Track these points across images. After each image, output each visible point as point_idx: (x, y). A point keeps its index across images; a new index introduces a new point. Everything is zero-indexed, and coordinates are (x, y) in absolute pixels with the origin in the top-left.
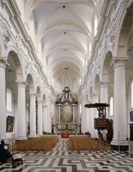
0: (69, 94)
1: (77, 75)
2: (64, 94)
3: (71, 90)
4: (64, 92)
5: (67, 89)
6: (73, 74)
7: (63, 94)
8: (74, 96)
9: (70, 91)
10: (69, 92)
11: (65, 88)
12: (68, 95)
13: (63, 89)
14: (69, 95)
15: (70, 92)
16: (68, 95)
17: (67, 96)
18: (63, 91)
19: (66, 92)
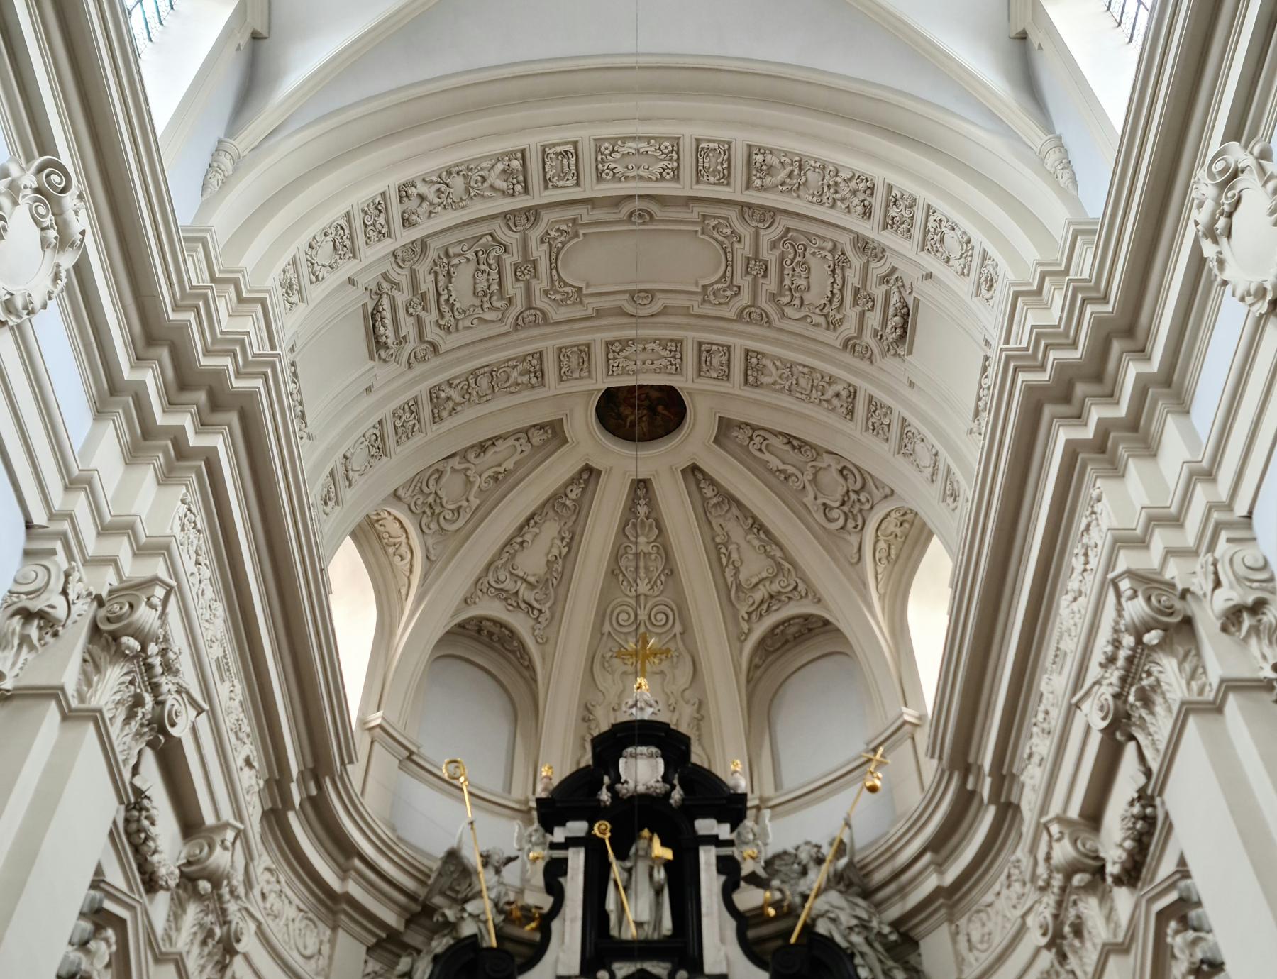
0: (707, 857)
1: (857, 493)
2: (577, 860)
3: (735, 774)
4: (577, 828)
5: (642, 771)
6: (758, 526)
7: (555, 872)
8: (835, 915)
9: (732, 807)
10: (705, 826)
11: (612, 744)
12: (681, 885)
13: (559, 759)
14: (710, 882)
15: (724, 831)
16: (681, 885)
17: (638, 909)
18: (551, 811)
19: (637, 815)
